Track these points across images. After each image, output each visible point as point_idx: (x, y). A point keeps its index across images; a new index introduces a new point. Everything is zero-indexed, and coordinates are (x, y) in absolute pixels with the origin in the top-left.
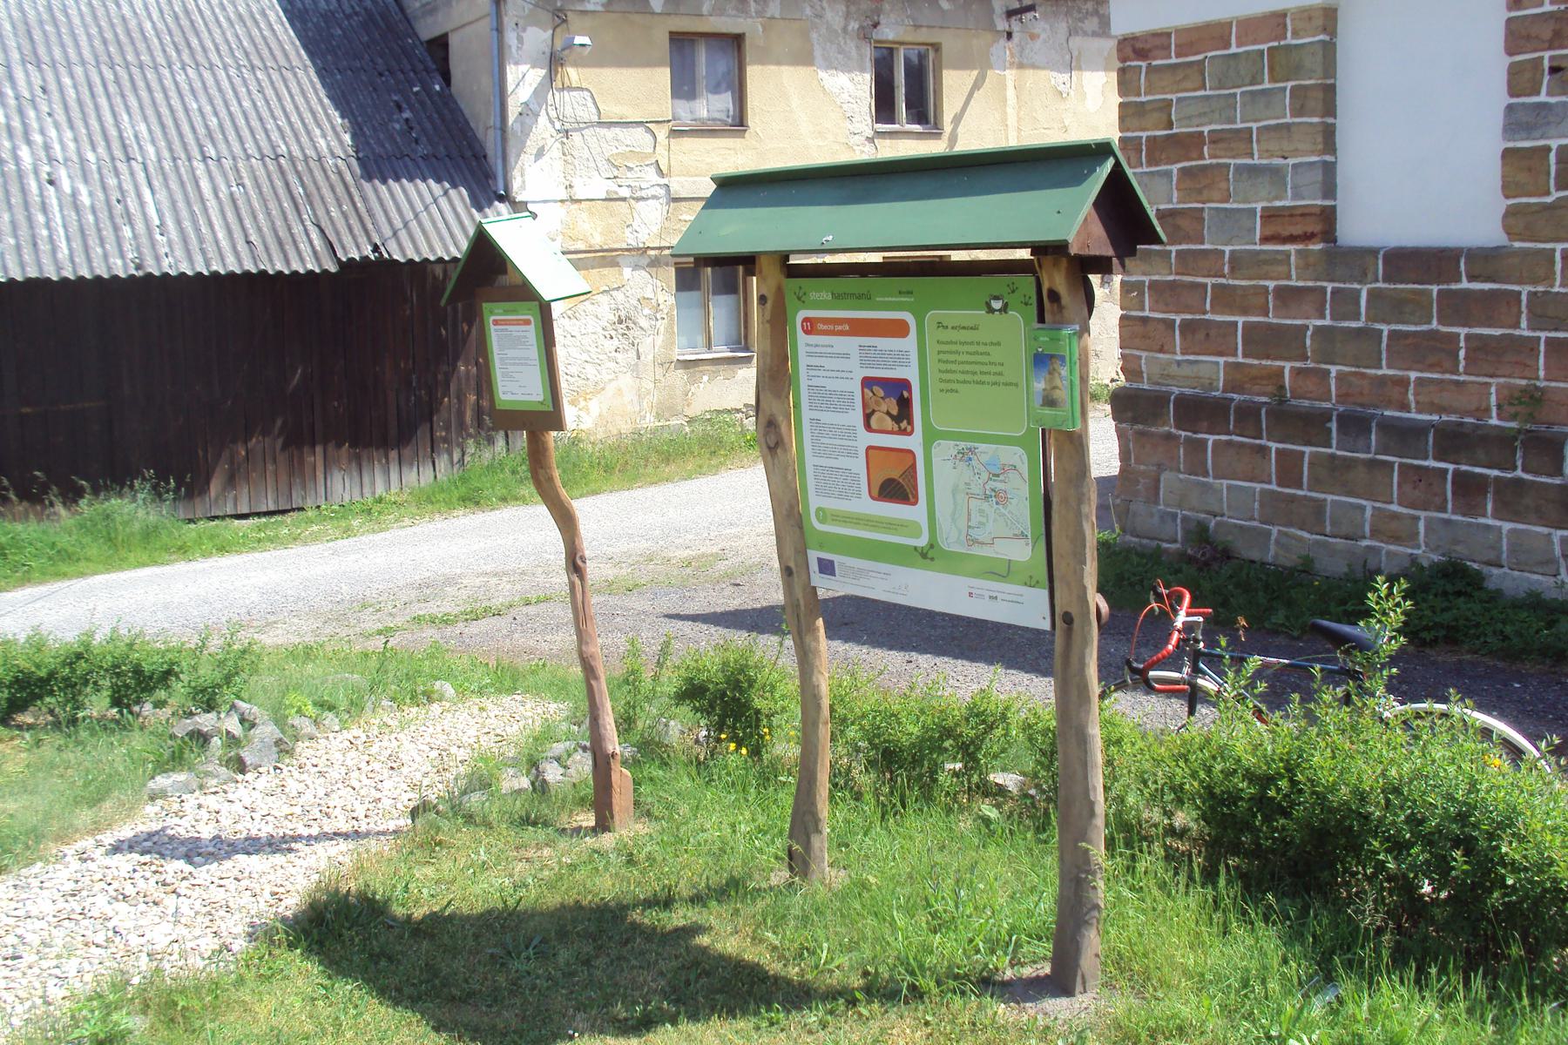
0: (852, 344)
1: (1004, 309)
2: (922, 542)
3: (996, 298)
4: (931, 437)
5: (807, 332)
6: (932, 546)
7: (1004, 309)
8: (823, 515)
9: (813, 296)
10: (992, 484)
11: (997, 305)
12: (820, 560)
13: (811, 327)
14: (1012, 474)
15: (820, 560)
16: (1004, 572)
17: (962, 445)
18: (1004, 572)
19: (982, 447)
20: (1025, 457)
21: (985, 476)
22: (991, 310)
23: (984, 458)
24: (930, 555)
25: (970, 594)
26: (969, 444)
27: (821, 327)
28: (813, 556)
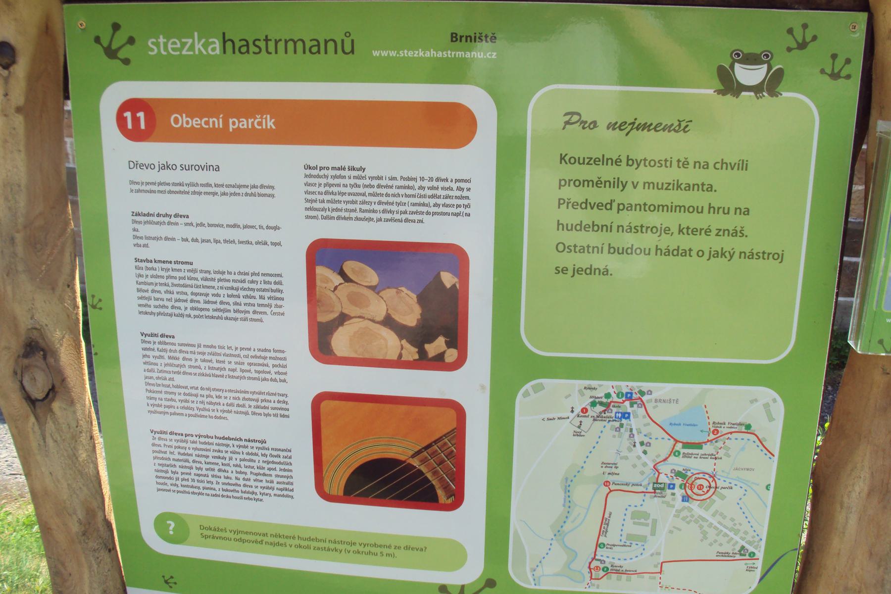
0: (284, 165)
1: (772, 85)
3: (751, 59)
4: (516, 368)
5: (135, 135)
8: (174, 526)
9: (159, 46)
10: (678, 463)
13: (144, 121)
14: (736, 443)
17: (605, 387)
19: (662, 389)
20: (779, 409)
21: (662, 446)
23: (661, 413)
26: (625, 386)
27: (184, 121)
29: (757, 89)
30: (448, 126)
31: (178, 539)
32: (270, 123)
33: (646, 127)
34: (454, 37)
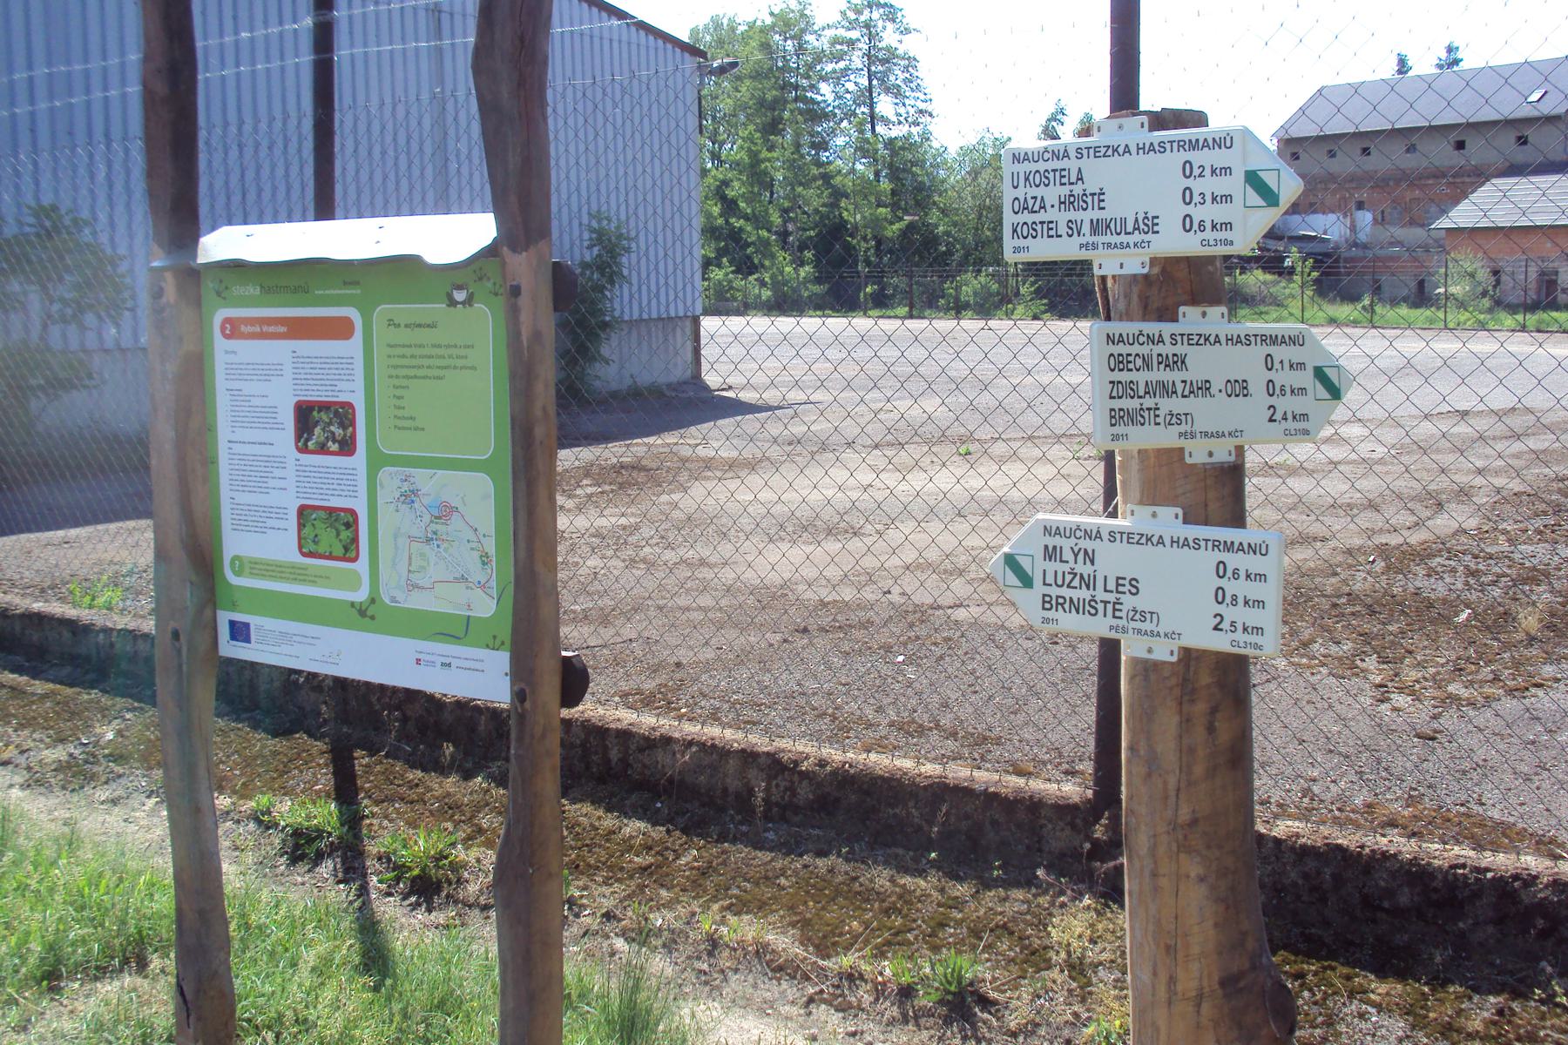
0: (281, 350)
1: (469, 301)
2: (361, 596)
3: (460, 288)
4: (377, 461)
5: (227, 337)
6: (373, 601)
7: (469, 301)
8: (240, 565)
9: (238, 291)
11: (460, 296)
12: (232, 624)
13: (233, 330)
15: (232, 624)
16: (459, 630)
18: (459, 630)
22: (453, 303)
24: (369, 613)
25: (418, 661)
27: (250, 329)
28: (224, 618)
29: (463, 303)
30: (340, 330)
31: (238, 574)
32: (282, 329)
33: (420, 326)
34: (345, 283)
